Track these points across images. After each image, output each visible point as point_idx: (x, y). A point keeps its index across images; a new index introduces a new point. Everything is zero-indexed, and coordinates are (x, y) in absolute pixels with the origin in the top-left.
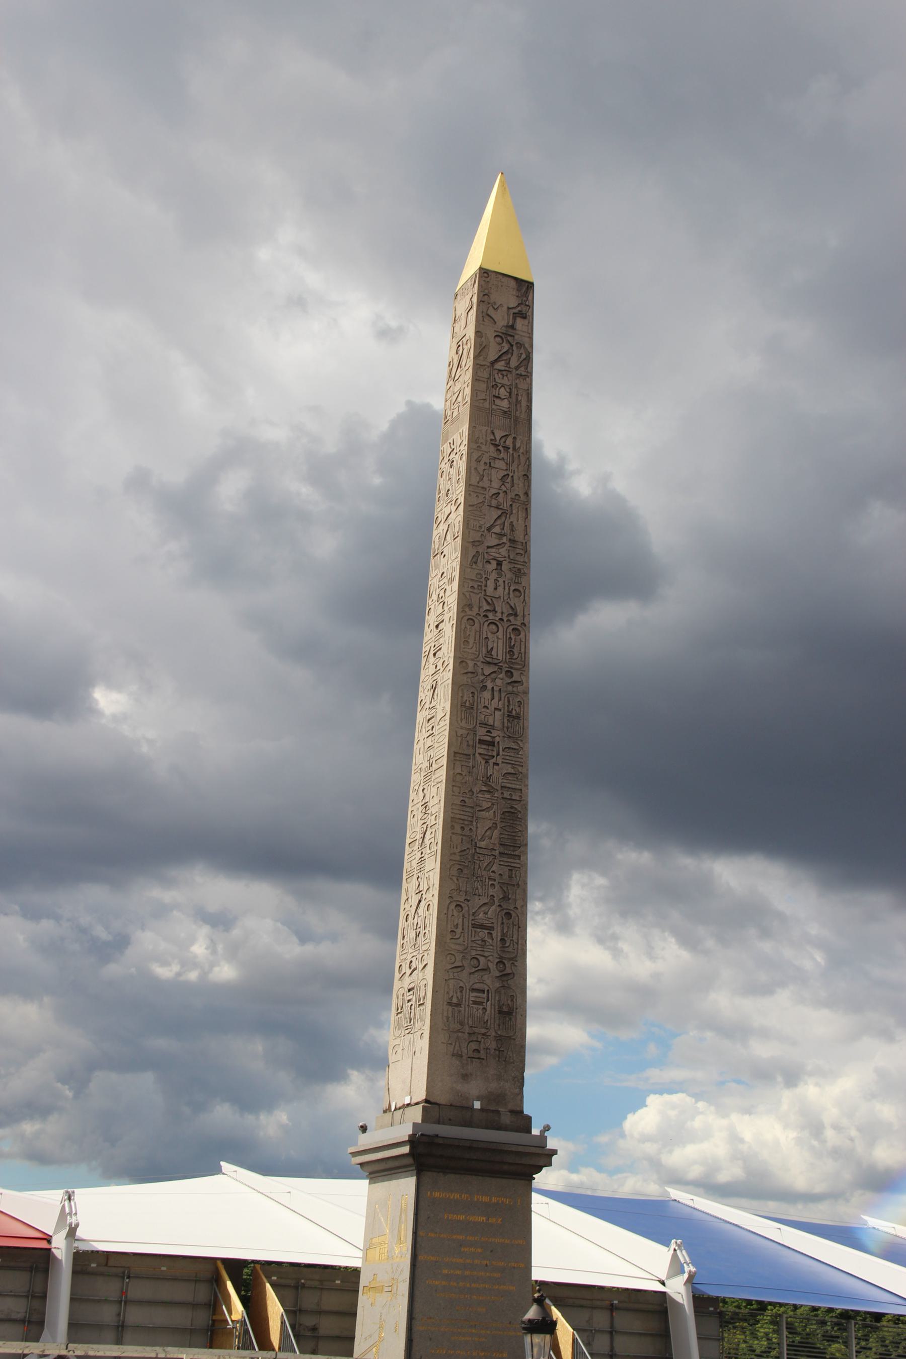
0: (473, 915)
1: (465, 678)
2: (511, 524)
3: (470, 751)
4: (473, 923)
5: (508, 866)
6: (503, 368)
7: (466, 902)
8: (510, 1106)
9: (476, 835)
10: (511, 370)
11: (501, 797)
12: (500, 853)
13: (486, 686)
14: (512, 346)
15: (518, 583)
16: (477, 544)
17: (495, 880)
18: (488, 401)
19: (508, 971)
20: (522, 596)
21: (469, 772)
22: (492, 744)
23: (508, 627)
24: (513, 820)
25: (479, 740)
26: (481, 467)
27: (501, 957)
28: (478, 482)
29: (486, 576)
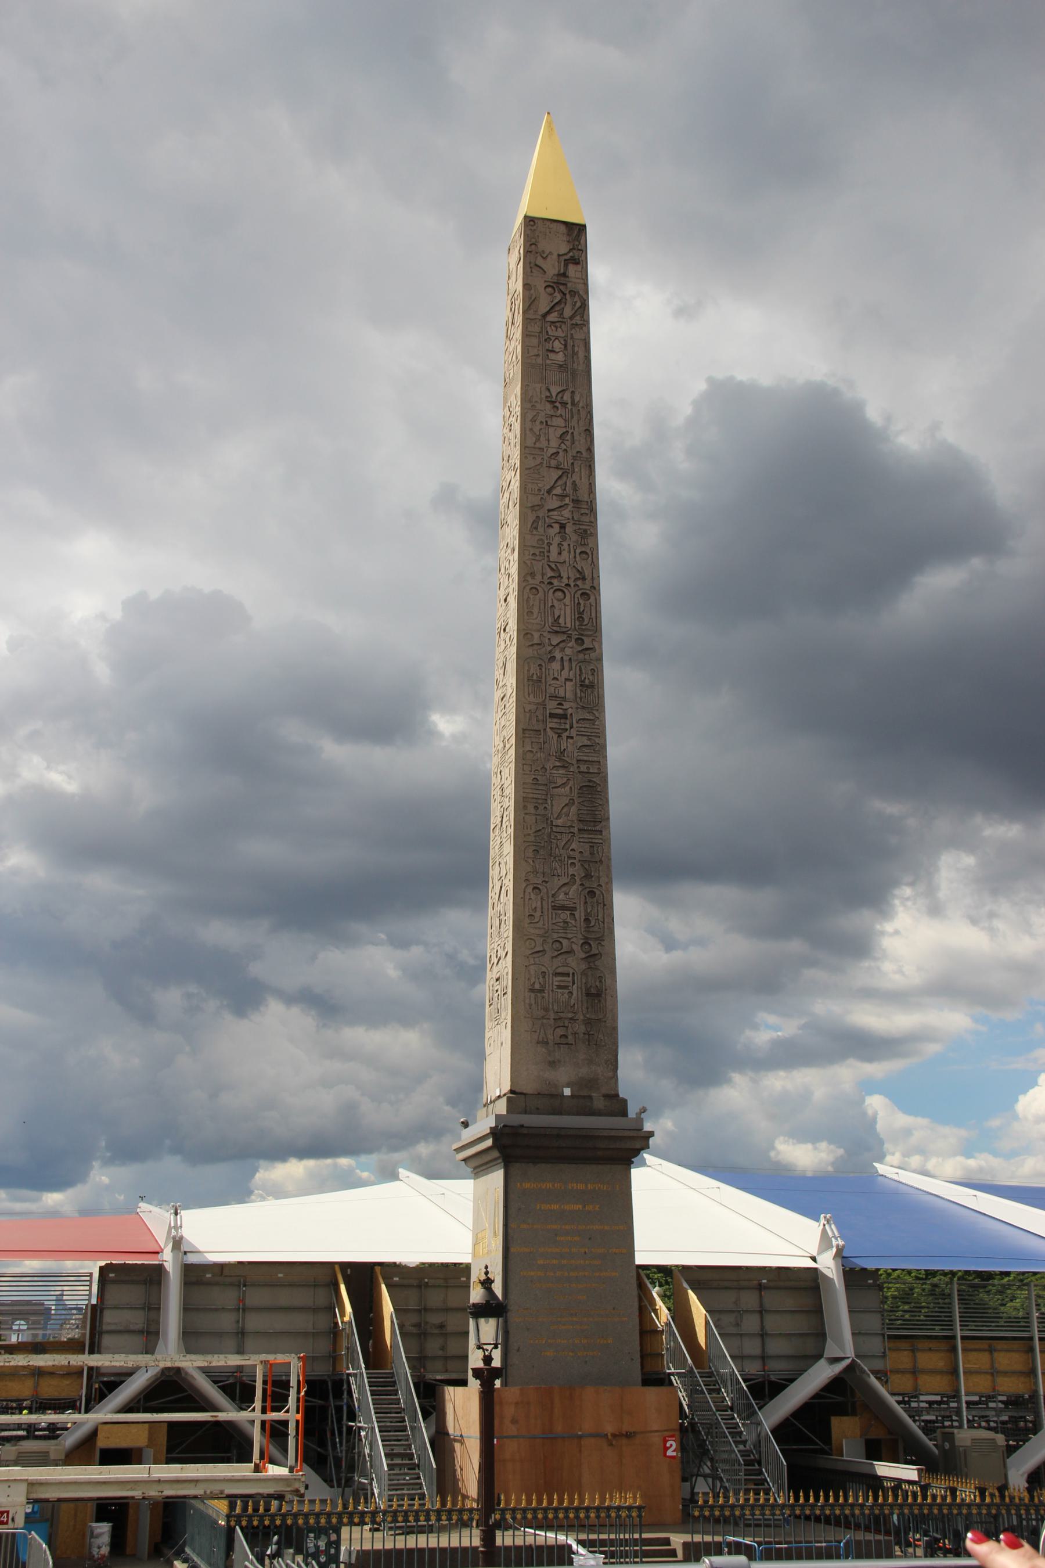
0: (553, 897)
2: (574, 483)
3: (541, 727)
4: (553, 904)
5: (590, 842)
6: (556, 320)
9: (552, 813)
10: (565, 320)
11: (577, 771)
12: (580, 830)
13: (554, 657)
14: (565, 294)
15: (585, 544)
16: (536, 508)
17: (575, 858)
18: (541, 357)
19: (594, 951)
20: (590, 559)
21: (541, 749)
22: (564, 716)
23: (576, 592)
24: (591, 794)
25: (550, 714)
26: (537, 428)
27: (586, 938)
29: (548, 541)
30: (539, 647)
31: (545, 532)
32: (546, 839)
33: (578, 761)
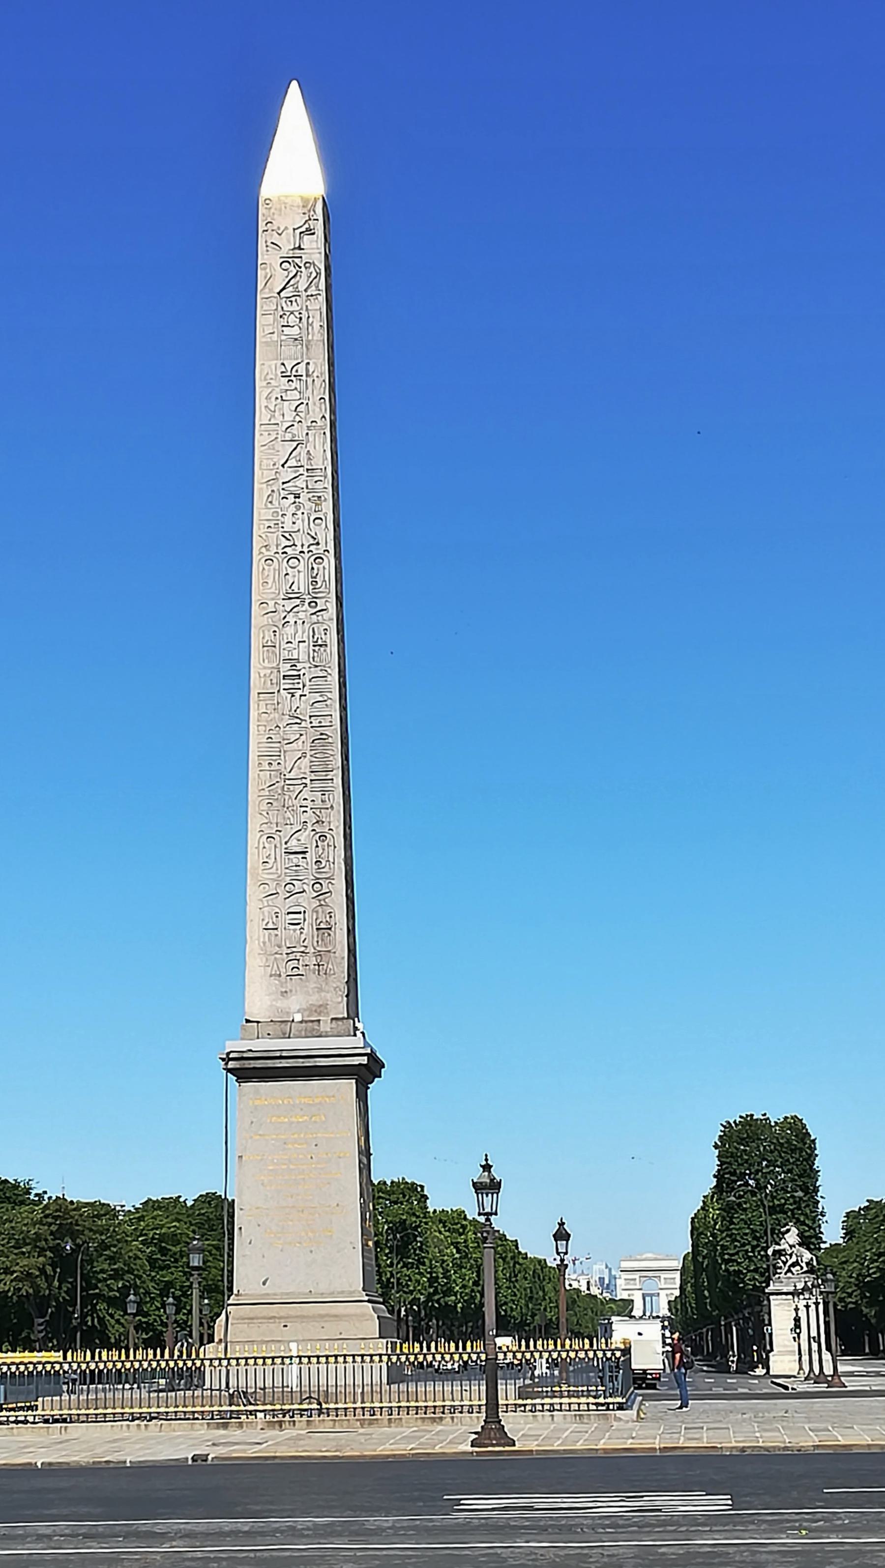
7: (278, 833)
10: (300, 294)
14: (300, 267)
15: (319, 511)
17: (307, 807)
25: (284, 676)
28: (270, 420)
32: (280, 792)
33: (310, 717)
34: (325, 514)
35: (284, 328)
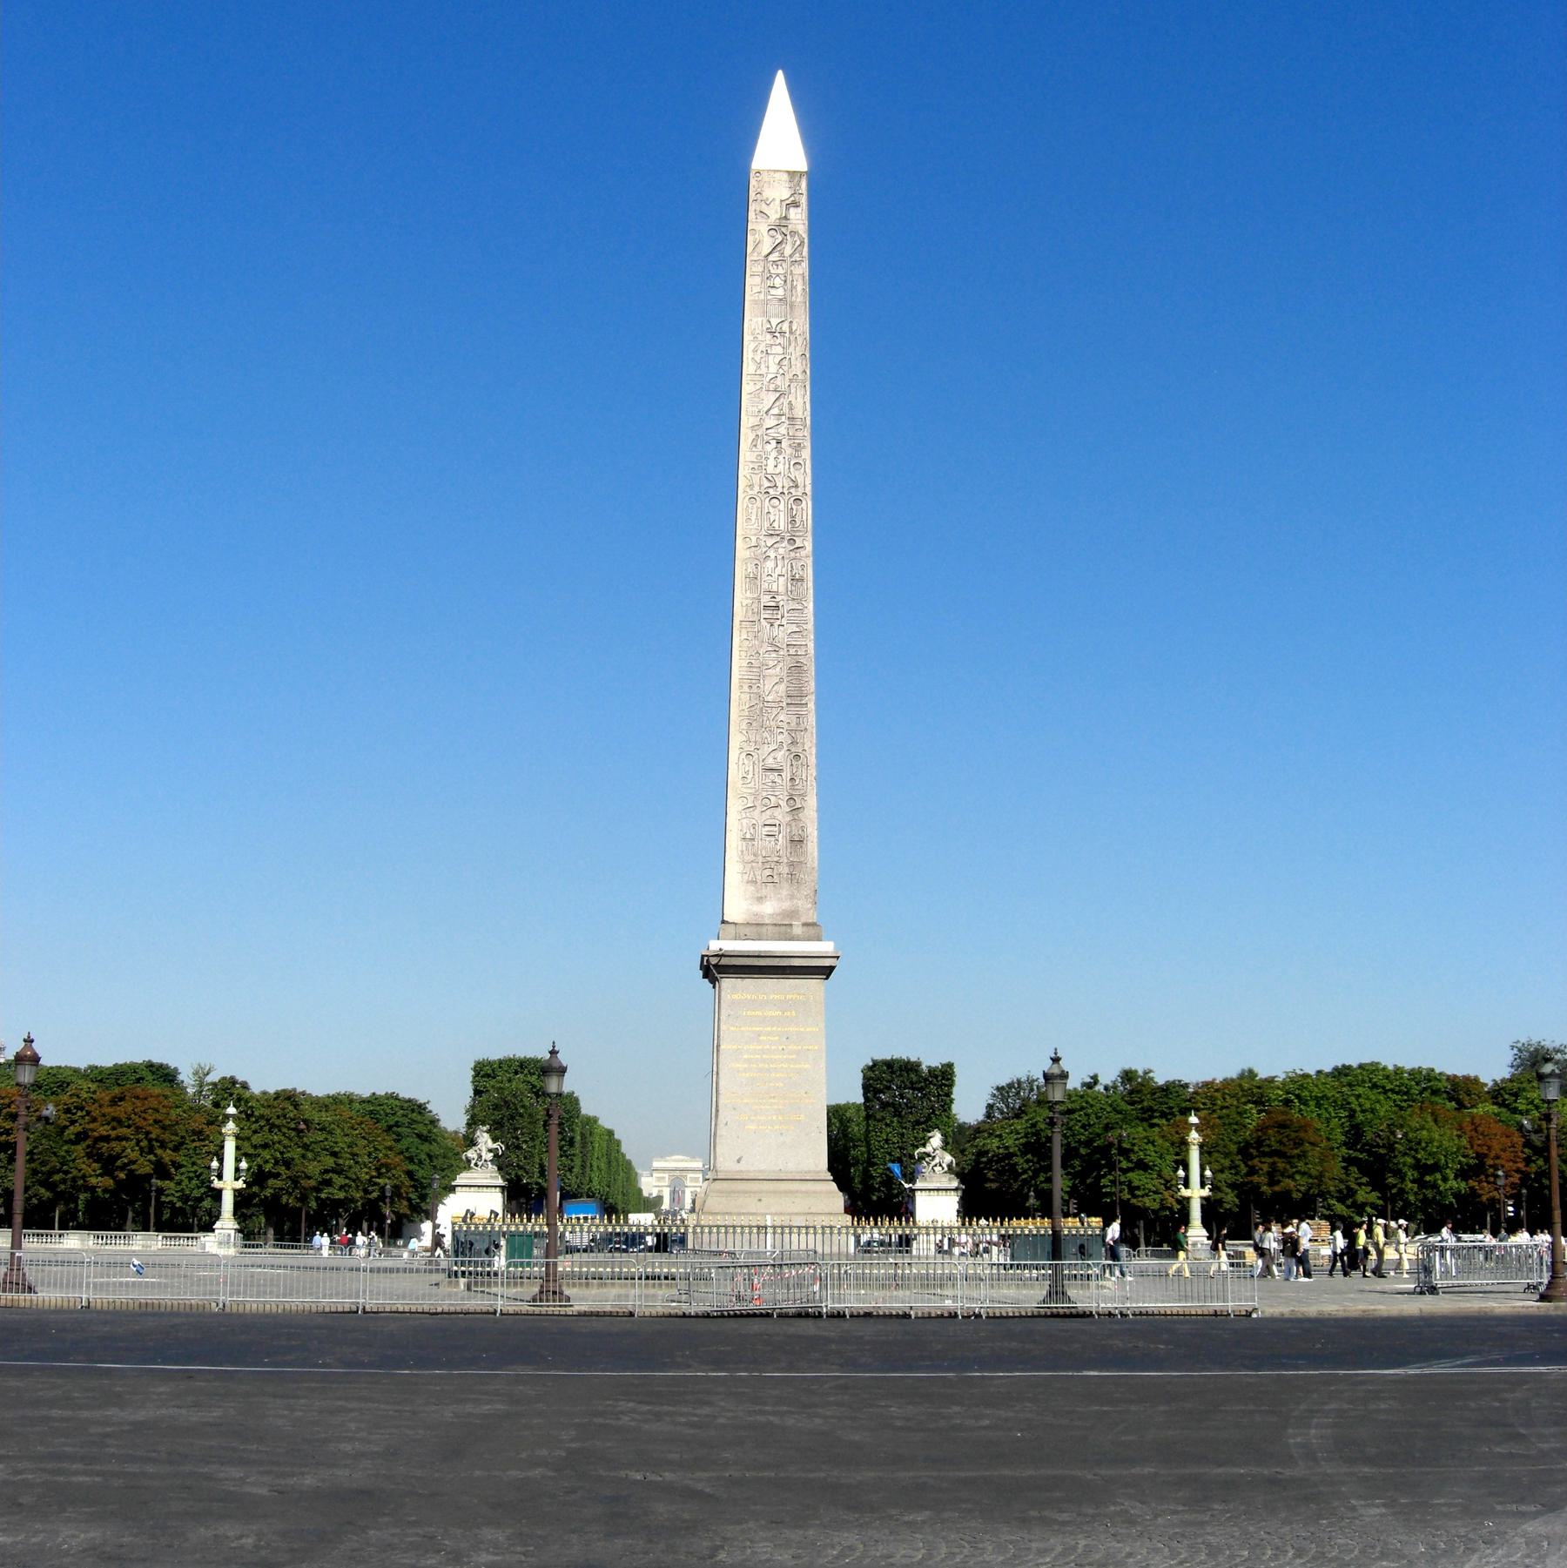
0: (763, 761)
1: (748, 553)
6: (778, 259)
8: (804, 919)
14: (786, 235)
16: (756, 428)
27: (792, 795)
30: (756, 549)
31: (763, 448)
34: (804, 460)
35: (770, 289)
